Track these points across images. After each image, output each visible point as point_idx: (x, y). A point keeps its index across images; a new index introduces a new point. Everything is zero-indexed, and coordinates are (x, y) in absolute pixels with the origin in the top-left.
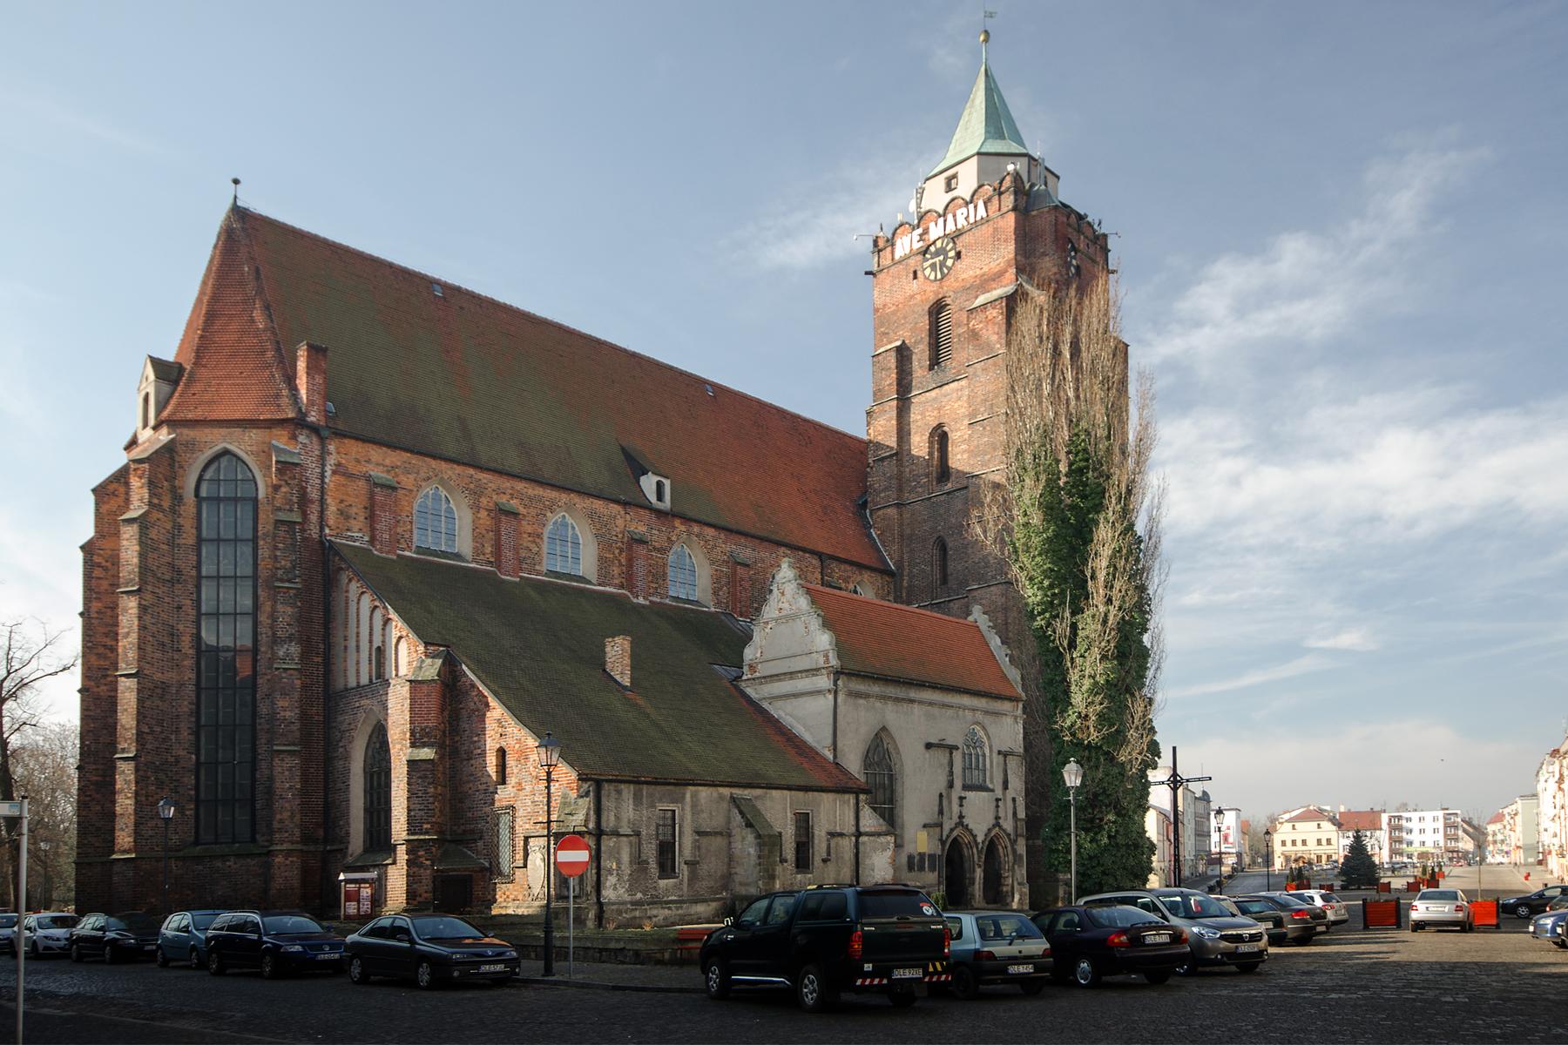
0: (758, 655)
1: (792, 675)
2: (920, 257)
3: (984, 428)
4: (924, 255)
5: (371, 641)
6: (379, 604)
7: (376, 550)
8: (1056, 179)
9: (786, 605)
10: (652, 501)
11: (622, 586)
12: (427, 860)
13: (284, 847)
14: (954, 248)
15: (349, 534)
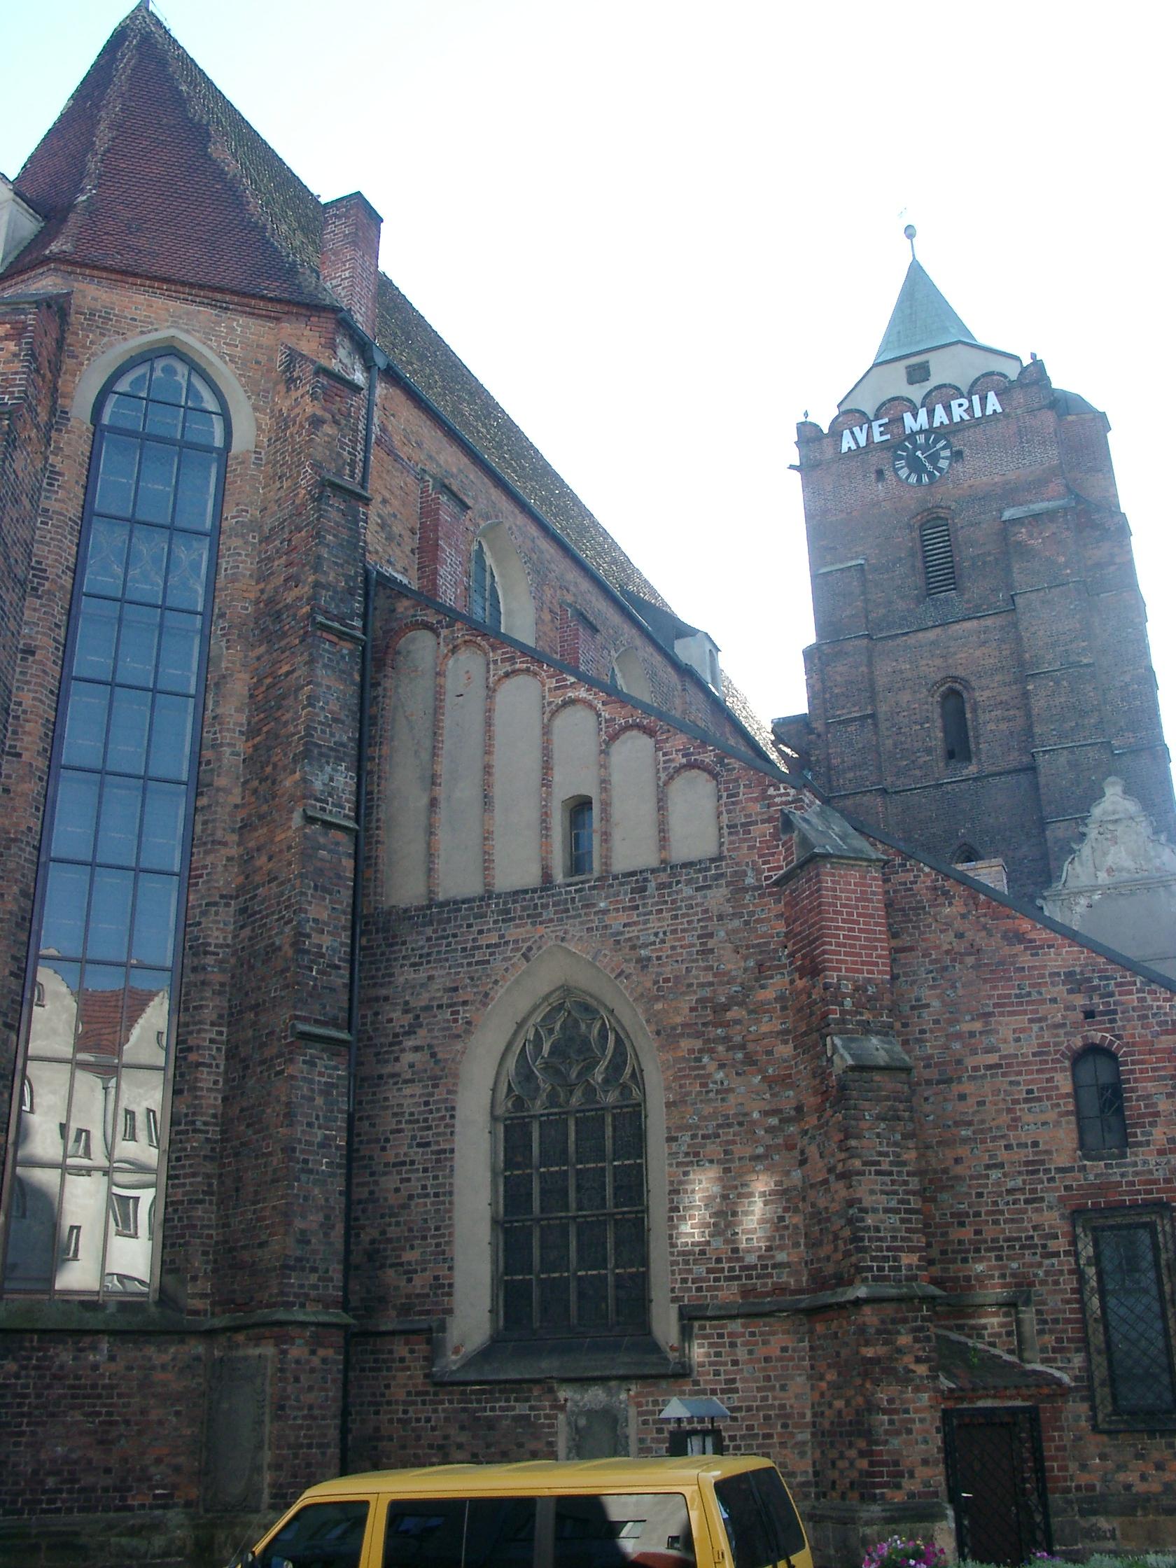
2: (887, 455)
3: (1057, 683)
12: (918, 1360)
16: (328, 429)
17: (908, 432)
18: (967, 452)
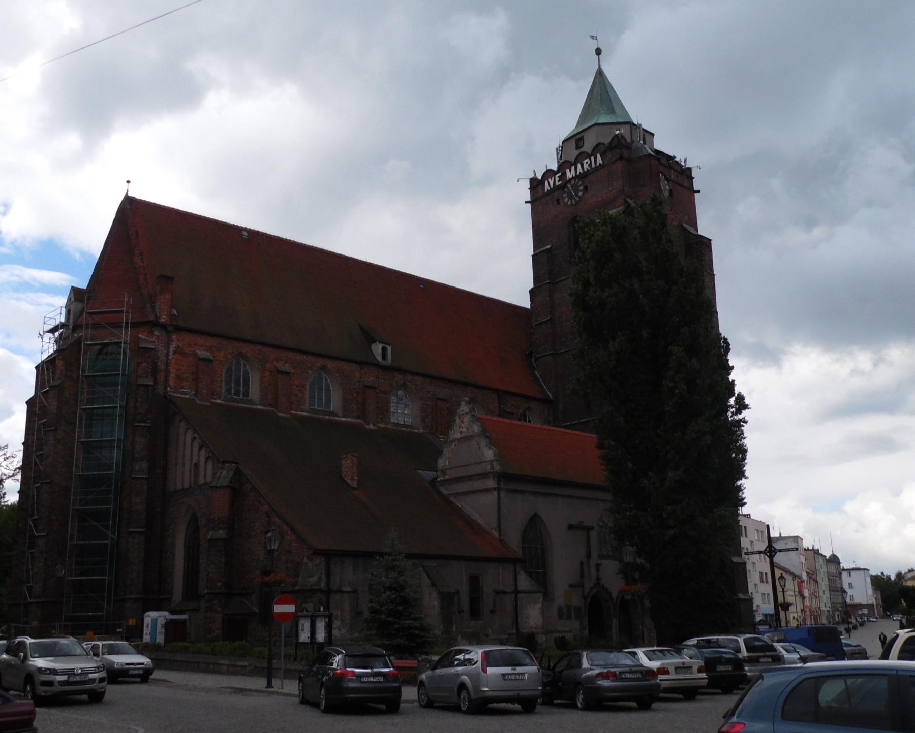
0: (447, 463)
1: (470, 478)
4: (563, 189)
5: (191, 460)
6: (196, 436)
7: (199, 400)
8: (652, 136)
9: (464, 430)
10: (379, 360)
11: (358, 417)
13: (132, 596)
14: (583, 184)
15: (182, 390)
16: (143, 365)
17: (568, 178)
18: (589, 186)
